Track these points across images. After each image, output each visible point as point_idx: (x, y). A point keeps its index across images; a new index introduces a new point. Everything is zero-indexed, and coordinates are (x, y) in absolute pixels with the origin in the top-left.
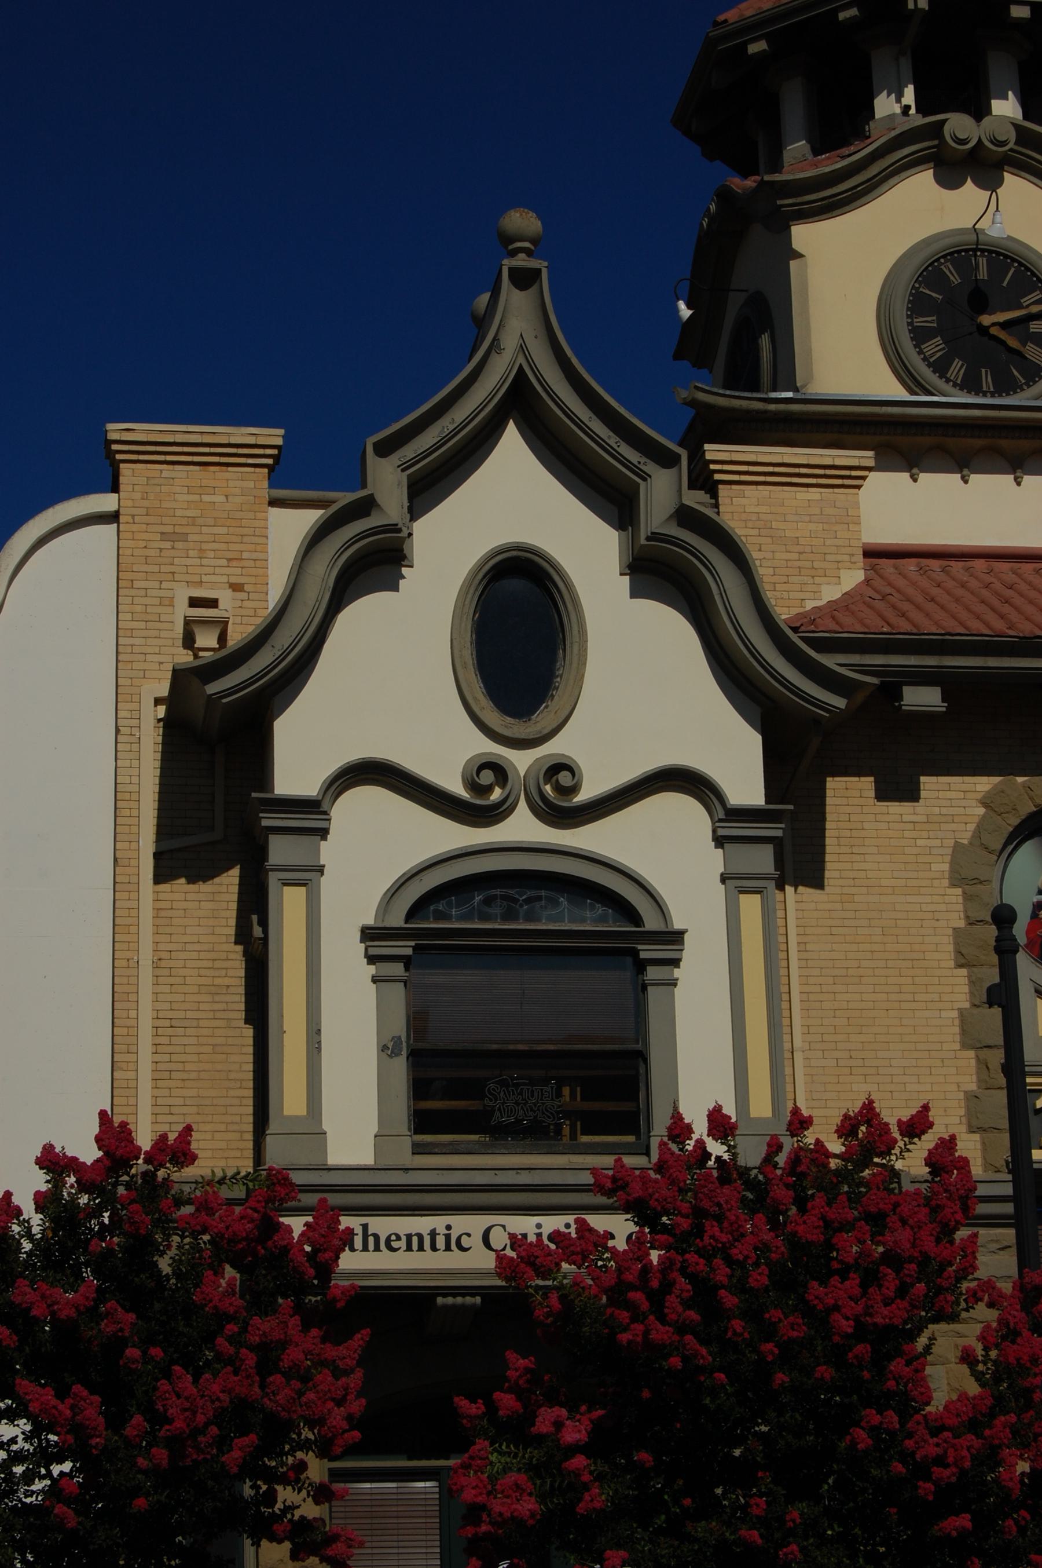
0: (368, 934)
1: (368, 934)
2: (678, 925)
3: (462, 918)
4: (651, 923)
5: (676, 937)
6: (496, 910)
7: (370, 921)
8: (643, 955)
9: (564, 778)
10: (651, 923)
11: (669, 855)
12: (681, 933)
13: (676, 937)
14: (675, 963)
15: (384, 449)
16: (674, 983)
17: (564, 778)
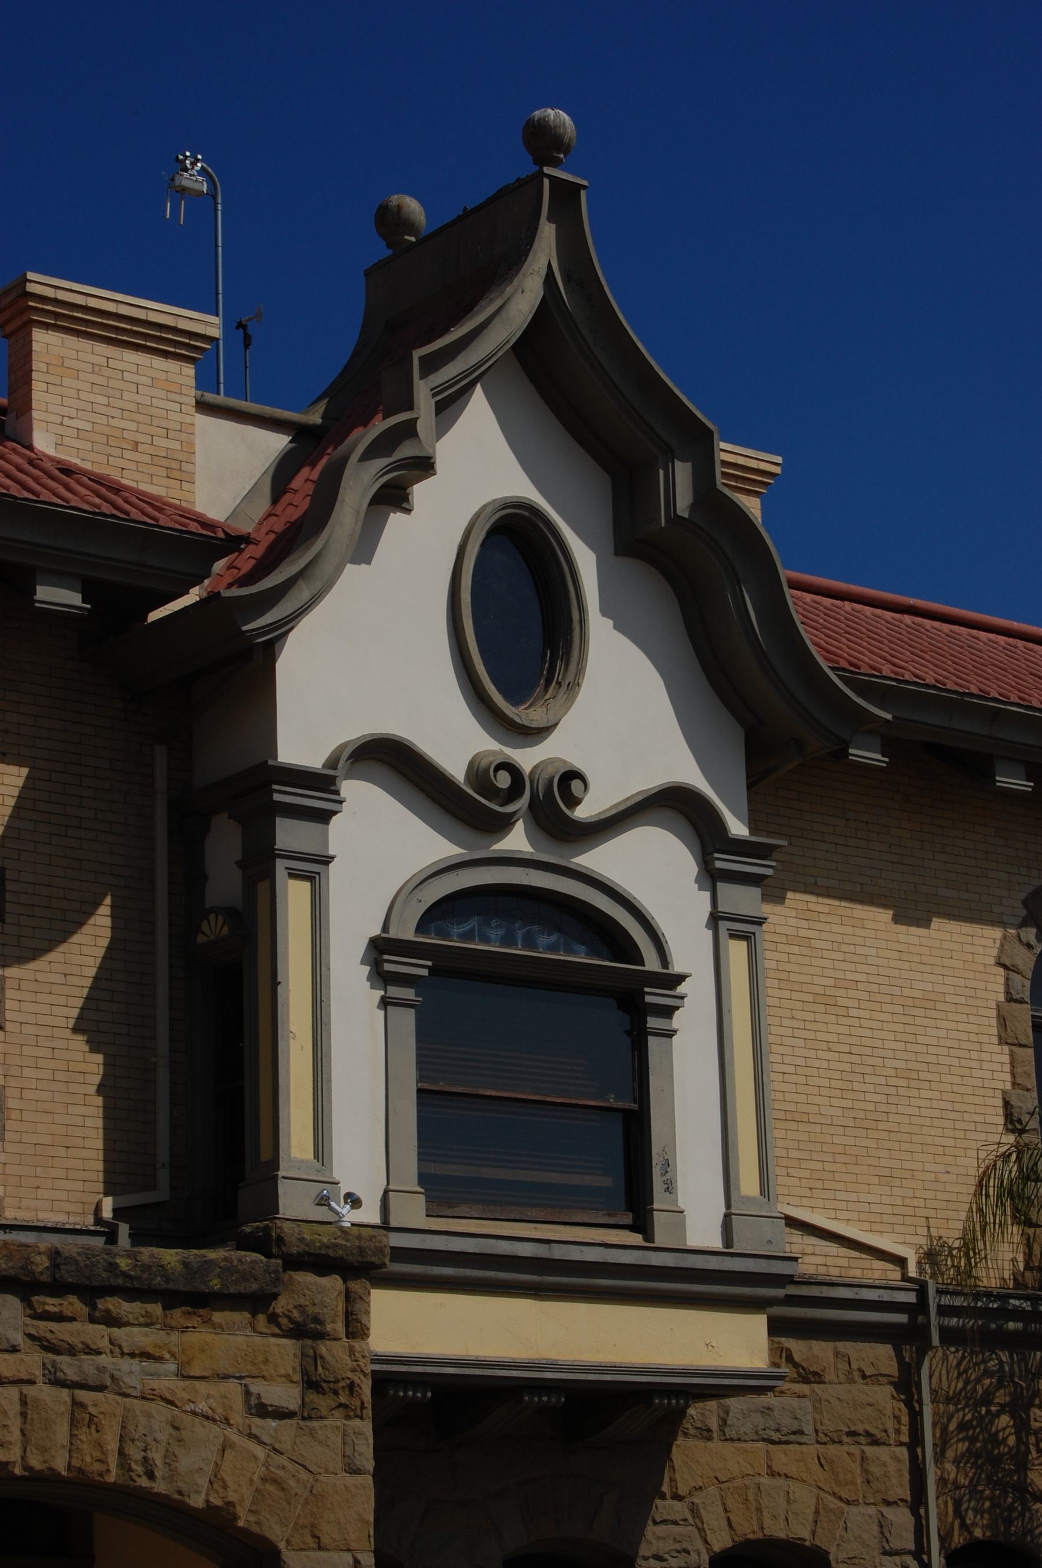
4: (652, 963)
10: (652, 963)
12: (681, 978)
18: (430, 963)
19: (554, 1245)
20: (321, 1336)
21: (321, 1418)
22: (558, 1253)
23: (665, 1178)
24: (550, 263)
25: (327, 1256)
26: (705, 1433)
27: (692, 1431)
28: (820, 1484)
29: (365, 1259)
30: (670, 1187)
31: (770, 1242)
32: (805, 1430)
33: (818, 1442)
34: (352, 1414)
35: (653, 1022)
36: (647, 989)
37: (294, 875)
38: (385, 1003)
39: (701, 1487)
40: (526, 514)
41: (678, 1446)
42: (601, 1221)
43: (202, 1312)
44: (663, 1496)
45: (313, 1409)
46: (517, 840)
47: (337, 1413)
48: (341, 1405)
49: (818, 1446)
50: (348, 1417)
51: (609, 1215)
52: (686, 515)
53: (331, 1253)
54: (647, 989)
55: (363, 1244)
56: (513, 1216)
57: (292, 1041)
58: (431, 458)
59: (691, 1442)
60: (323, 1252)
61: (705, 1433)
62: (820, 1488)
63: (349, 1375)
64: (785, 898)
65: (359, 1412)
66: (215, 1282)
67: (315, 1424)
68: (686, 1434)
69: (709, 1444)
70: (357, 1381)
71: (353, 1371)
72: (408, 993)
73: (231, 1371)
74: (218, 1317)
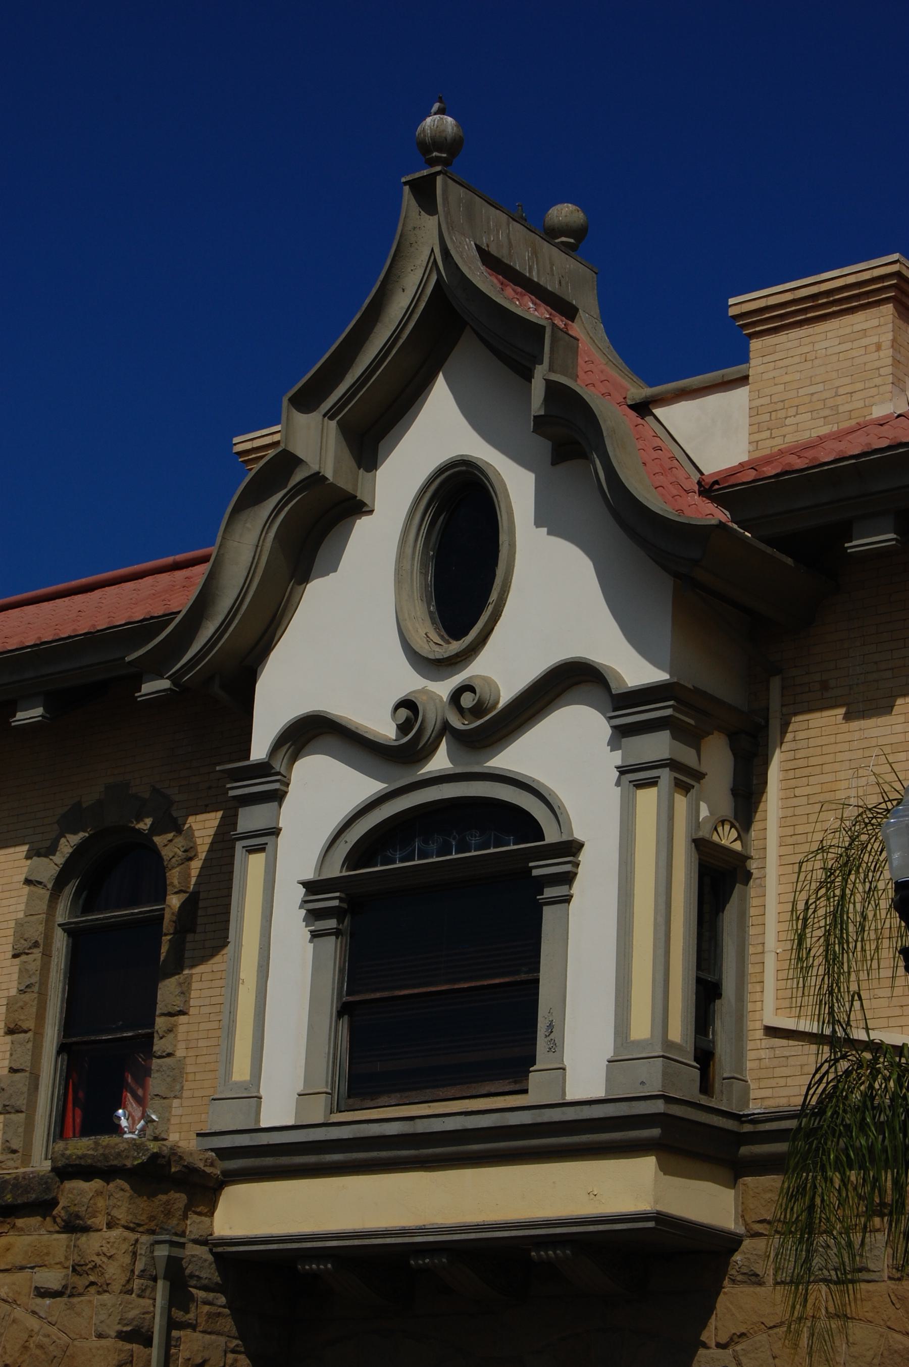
0: (311, 887)
1: (311, 887)
2: (578, 835)
3: (402, 861)
4: (551, 836)
5: (572, 848)
6: (433, 847)
7: (309, 875)
8: (535, 872)
9: (467, 700)
10: (551, 836)
11: (568, 763)
13: (572, 848)
14: (568, 878)
15: (306, 401)
16: (567, 899)
17: (467, 700)
18: (337, 894)
19: (418, 1120)
20: (86, 1229)
21: (80, 1295)
22: (421, 1127)
23: (549, 1038)
24: (432, 250)
25: (80, 1165)
26: (753, 1279)
27: (740, 1278)
28: (889, 1324)
29: (109, 1164)
30: (556, 1047)
31: (643, 1083)
32: (871, 1266)
33: (890, 1278)
34: (100, 1290)
35: (550, 892)
36: (531, 864)
37: (252, 850)
38: (315, 935)
39: (743, 1335)
40: (464, 468)
41: (725, 1293)
42: (507, 1089)
43: (8, 1220)
44: (705, 1346)
45: (74, 1288)
46: (440, 761)
47: (92, 1290)
48: (92, 1284)
49: (889, 1282)
50: (99, 1293)
51: (516, 1082)
52: (542, 413)
53: (83, 1162)
54: (531, 864)
55: (107, 1152)
56: (426, 1099)
57: (241, 986)
58: (319, 473)
59: (739, 1289)
60: (77, 1162)
61: (755, 1279)
62: (889, 1328)
63: (95, 1258)
64: (892, 707)
65: (105, 1287)
66: (8, 1196)
67: (75, 1300)
68: (733, 1281)
69: (758, 1289)
70: (99, 1262)
71: (98, 1255)
72: (332, 923)
73: (24, 1263)
74: (20, 1222)
